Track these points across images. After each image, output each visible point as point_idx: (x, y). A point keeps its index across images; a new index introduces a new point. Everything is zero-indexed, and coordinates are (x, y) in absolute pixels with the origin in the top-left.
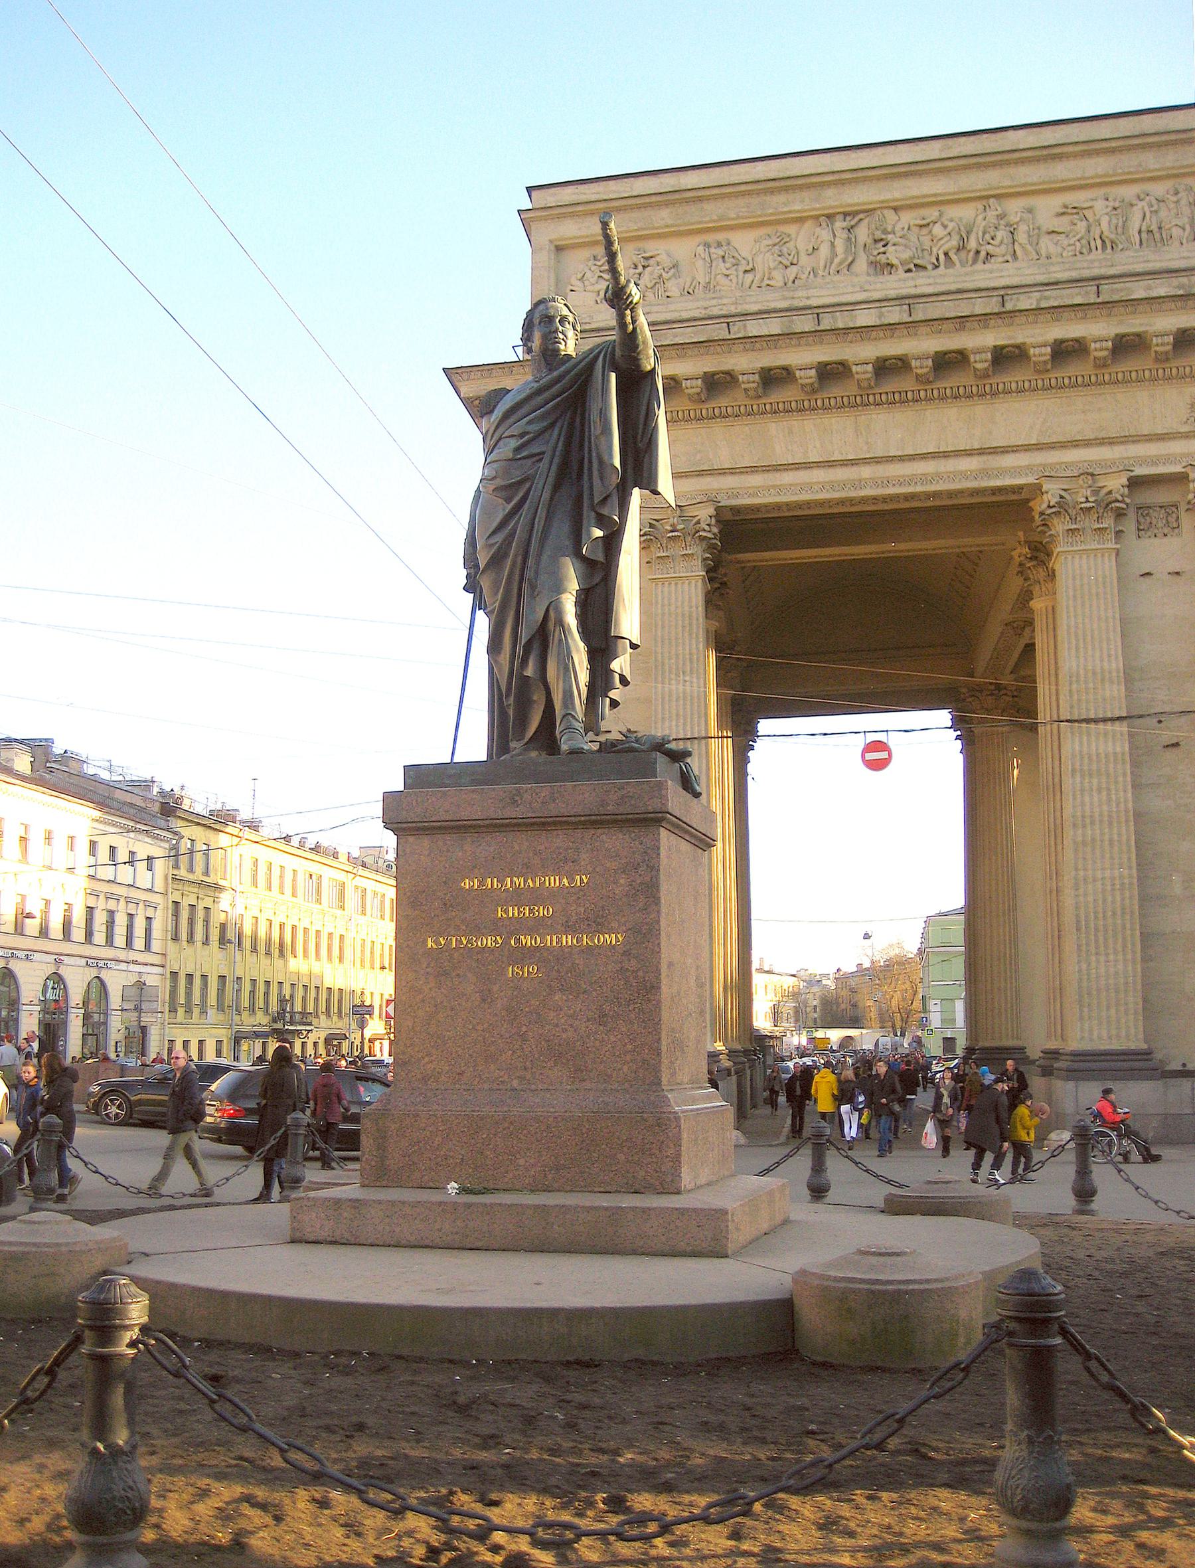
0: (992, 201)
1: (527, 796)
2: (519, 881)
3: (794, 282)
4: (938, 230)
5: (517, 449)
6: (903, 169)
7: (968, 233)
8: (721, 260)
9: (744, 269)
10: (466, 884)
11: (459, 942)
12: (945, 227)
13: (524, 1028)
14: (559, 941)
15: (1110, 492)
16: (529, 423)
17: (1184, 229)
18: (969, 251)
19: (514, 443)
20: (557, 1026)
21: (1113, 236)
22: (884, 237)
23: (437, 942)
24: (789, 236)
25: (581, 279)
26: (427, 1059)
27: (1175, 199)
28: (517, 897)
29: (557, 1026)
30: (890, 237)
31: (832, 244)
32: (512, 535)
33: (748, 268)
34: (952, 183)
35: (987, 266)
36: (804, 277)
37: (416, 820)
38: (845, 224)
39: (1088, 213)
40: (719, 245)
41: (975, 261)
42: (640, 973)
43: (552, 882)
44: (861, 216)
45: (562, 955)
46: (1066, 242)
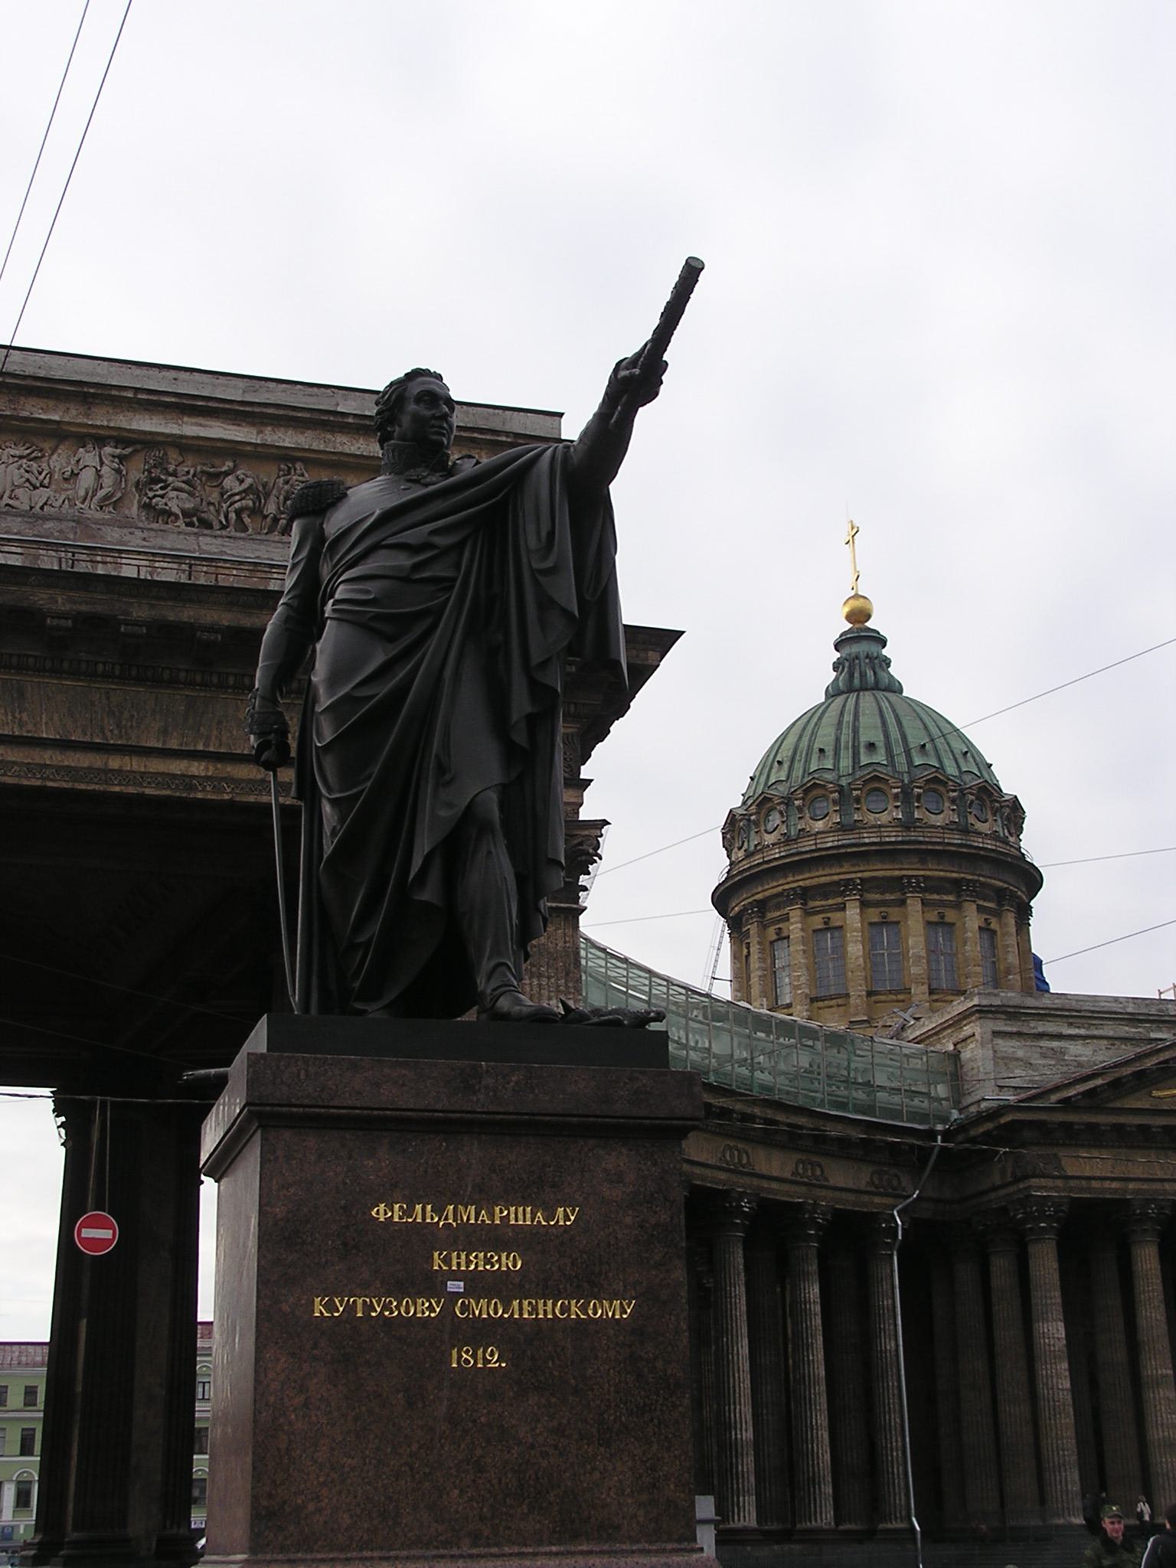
0: (298, 465)
1: (489, 1081)
2: (469, 1214)
3: (42, 508)
4: (229, 482)
5: (416, 567)
7: (267, 495)
10: (380, 1212)
12: (242, 481)
13: (479, 1452)
14: (534, 1309)
16: (433, 533)
18: (265, 517)
19: (404, 561)
20: (532, 1446)
22: (163, 477)
23: (331, 1307)
26: (311, 1507)
29: (532, 1446)
31: (98, 475)
34: (255, 432)
36: (57, 504)
37: (306, 1102)
41: (271, 531)
42: (659, 1364)
43: (521, 1216)
44: (138, 447)
45: (540, 1330)
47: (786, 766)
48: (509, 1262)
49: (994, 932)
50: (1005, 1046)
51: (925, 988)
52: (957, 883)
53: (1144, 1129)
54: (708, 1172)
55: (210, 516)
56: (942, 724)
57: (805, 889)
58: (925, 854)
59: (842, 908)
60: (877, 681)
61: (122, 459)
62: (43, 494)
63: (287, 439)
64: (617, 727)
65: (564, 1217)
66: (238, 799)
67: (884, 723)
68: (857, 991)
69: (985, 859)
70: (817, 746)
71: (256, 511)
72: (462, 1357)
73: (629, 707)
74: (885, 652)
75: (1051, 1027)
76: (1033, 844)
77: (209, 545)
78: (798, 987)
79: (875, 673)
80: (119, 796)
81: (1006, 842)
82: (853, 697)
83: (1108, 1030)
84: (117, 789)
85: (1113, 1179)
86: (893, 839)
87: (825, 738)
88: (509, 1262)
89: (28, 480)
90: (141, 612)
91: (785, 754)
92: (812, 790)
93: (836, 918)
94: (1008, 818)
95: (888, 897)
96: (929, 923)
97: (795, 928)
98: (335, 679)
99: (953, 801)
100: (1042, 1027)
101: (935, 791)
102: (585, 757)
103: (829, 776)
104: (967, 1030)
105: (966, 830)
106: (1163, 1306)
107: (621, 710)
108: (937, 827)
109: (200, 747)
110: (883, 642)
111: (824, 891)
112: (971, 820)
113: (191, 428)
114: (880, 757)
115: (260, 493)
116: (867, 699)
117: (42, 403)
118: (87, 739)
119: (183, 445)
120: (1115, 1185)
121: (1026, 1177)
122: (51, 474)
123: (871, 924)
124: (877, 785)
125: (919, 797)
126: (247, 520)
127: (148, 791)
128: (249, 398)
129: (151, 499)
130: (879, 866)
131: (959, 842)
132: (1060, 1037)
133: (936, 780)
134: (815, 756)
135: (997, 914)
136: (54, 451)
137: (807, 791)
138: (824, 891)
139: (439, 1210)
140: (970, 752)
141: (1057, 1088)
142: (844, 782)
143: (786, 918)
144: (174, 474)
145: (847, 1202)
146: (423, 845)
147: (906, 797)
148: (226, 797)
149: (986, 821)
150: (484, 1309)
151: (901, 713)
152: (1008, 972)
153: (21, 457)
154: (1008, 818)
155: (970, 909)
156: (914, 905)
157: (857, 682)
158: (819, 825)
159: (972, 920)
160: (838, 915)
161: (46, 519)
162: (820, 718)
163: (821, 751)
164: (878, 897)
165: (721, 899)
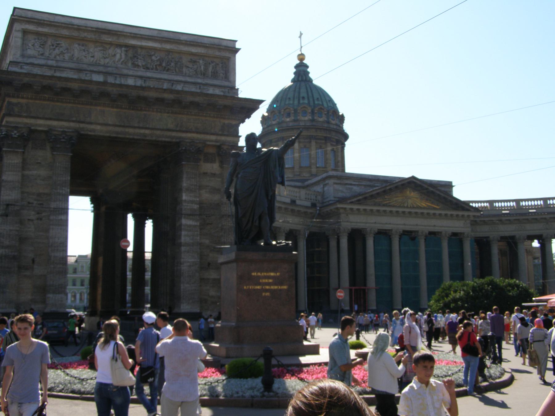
2: (265, 274)
3: (107, 64)
4: (153, 58)
6: (146, 37)
7: (163, 61)
8: (83, 51)
9: (90, 55)
10: (253, 274)
11: (252, 287)
15: (199, 148)
17: (223, 74)
21: (204, 72)
22: (137, 56)
23: (246, 287)
25: (33, 45)
27: (222, 65)
28: (266, 277)
30: (139, 57)
31: (121, 55)
33: (93, 55)
35: (168, 73)
36: (111, 63)
38: (126, 49)
39: (198, 64)
40: (83, 45)
41: (164, 71)
43: (272, 274)
45: (275, 290)
46: (191, 71)
48: (271, 281)
49: (335, 152)
50: (336, 186)
55: (149, 66)
57: (283, 137)
60: (306, 78)
62: (107, 61)
63: (168, 46)
64: (247, 120)
65: (278, 274)
67: (307, 92)
72: (263, 294)
76: (347, 127)
81: (339, 126)
83: (364, 183)
86: (308, 124)
87: (291, 95)
88: (271, 281)
89: (103, 57)
99: (325, 114)
104: (327, 182)
105: (328, 122)
107: (249, 117)
108: (320, 122)
109: (147, 126)
110: (307, 67)
112: (330, 120)
115: (161, 60)
116: (303, 84)
119: (142, 47)
122: (109, 54)
125: (316, 113)
126: (158, 67)
128: (159, 36)
129: (134, 62)
131: (326, 126)
132: (351, 184)
136: (109, 48)
137: (285, 110)
139: (261, 273)
140: (331, 100)
141: (350, 198)
142: (295, 108)
144: (140, 55)
145: (294, 227)
149: (334, 120)
150: (267, 287)
152: (338, 162)
153: (101, 50)
156: (313, 143)
158: (288, 120)
161: (109, 67)
163: (289, 98)
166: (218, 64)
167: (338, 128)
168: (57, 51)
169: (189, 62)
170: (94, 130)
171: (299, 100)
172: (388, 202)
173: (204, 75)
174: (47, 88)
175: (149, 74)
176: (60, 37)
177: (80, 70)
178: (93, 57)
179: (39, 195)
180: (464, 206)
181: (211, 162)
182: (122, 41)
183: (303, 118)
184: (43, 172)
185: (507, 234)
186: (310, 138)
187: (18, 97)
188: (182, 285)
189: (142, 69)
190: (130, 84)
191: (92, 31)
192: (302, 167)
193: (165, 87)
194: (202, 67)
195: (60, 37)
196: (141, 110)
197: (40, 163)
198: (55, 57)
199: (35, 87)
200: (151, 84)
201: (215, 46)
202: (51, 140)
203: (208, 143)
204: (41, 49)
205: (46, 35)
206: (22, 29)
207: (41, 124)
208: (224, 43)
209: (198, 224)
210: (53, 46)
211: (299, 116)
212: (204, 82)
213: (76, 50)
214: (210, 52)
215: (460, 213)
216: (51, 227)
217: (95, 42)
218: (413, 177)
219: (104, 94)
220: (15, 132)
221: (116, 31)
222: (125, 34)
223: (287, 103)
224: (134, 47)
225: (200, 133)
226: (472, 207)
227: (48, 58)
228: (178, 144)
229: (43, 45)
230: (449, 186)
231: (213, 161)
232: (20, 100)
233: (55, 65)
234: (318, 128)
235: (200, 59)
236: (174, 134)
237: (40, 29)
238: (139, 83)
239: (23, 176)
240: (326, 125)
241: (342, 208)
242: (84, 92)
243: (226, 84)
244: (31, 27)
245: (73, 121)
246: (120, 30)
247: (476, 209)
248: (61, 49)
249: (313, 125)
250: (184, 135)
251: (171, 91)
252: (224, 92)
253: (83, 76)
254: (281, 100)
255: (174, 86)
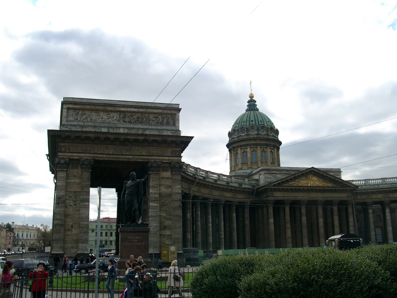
4: (134, 117)
6: (130, 106)
10: (128, 238)
24: (109, 113)
32: (130, 200)
40: (97, 113)
43: (137, 238)
47: (238, 124)
48: (137, 241)
49: (273, 152)
51: (260, 162)
52: (266, 144)
53: (287, 189)
54: (217, 197)
55: (132, 121)
56: (265, 116)
57: (241, 145)
58: (261, 140)
59: (247, 148)
60: (254, 109)
61: (120, 114)
62: (110, 120)
63: (142, 110)
66: (136, 160)
68: (249, 163)
69: (271, 140)
70: (243, 121)
71: (138, 120)
73: (188, 145)
74: (256, 103)
75: (274, 172)
77: (132, 126)
78: (239, 162)
79: (254, 107)
80: (121, 161)
81: (275, 137)
82: (250, 112)
83: (284, 172)
84: (120, 160)
85: (282, 197)
87: (245, 119)
88: (137, 241)
90: (122, 137)
91: (238, 122)
92: (242, 128)
93: (246, 150)
94: (276, 133)
95: (255, 147)
96: (261, 151)
97: (239, 152)
98: (127, 198)
99: (266, 130)
100: (273, 172)
101: (263, 128)
102: (182, 152)
103: (245, 126)
104: (261, 173)
105: (268, 135)
106: (289, 217)
109: (131, 154)
110: (256, 102)
111: (244, 146)
112: (269, 133)
113: (129, 109)
114: (254, 123)
115: (138, 118)
116: (252, 112)
117: (109, 107)
118: (116, 154)
119: (128, 112)
120: (282, 198)
121: (268, 197)
122: (111, 117)
123: (252, 151)
124: (253, 128)
125: (260, 130)
126: (136, 122)
127: (124, 160)
128: (137, 105)
130: (253, 141)
132: (276, 174)
133: (263, 127)
134: (243, 122)
135: (274, 149)
138: (244, 146)
140: (270, 121)
141: (273, 183)
143: (238, 150)
146: (132, 211)
147: (258, 130)
148: (134, 160)
151: (258, 115)
154: (276, 133)
155: (268, 148)
156: (259, 148)
157: (251, 109)
159: (269, 150)
160: (246, 150)
162: (244, 116)
163: (244, 122)
164: (253, 147)
165: (228, 146)
166: (169, 118)
167: (274, 138)
168: (84, 117)
169: (154, 117)
170: (102, 157)
171: (249, 123)
172: (296, 184)
173: (162, 124)
174: (78, 138)
175: (132, 126)
176: (85, 110)
177: (95, 127)
178: (102, 118)
179: (75, 192)
180: (347, 184)
181: (166, 171)
182: (117, 109)
183: (252, 133)
184: (77, 181)
185: (378, 200)
186: (256, 145)
187: (64, 142)
188: (150, 238)
189: (128, 124)
190: (121, 132)
191: (102, 105)
192: (253, 163)
193: (140, 133)
194: (161, 120)
195: (85, 110)
196: (127, 145)
197: (75, 176)
198: (83, 120)
199: (72, 137)
200: (133, 132)
201: (167, 108)
202: (80, 164)
203: (163, 161)
204: (76, 117)
205: (79, 109)
206: (67, 107)
207: (76, 156)
208: (173, 106)
209: (159, 205)
210: (82, 114)
211: (250, 132)
212: (161, 128)
213: (93, 116)
214: (165, 111)
215: (344, 188)
216: (81, 209)
217: (103, 111)
218: (313, 168)
219: (107, 139)
220: (63, 160)
221: (114, 104)
222: (119, 105)
223: (242, 124)
224: (123, 112)
225: (159, 156)
226: (353, 185)
227: (80, 121)
228: (147, 163)
229: (77, 114)
230: (339, 171)
231: (167, 171)
232: (65, 144)
233: (83, 125)
234: (261, 139)
235: (159, 116)
236: (145, 157)
237: (76, 107)
238: (126, 131)
239: (67, 183)
240: (266, 137)
241: (269, 188)
242: (97, 139)
243: (174, 128)
244: (71, 106)
245: (92, 153)
246: (116, 104)
247: (357, 187)
248: (86, 116)
249: (258, 137)
250: (150, 158)
251: (142, 135)
252: (173, 133)
253: (97, 130)
254: (239, 123)
255: (145, 131)
